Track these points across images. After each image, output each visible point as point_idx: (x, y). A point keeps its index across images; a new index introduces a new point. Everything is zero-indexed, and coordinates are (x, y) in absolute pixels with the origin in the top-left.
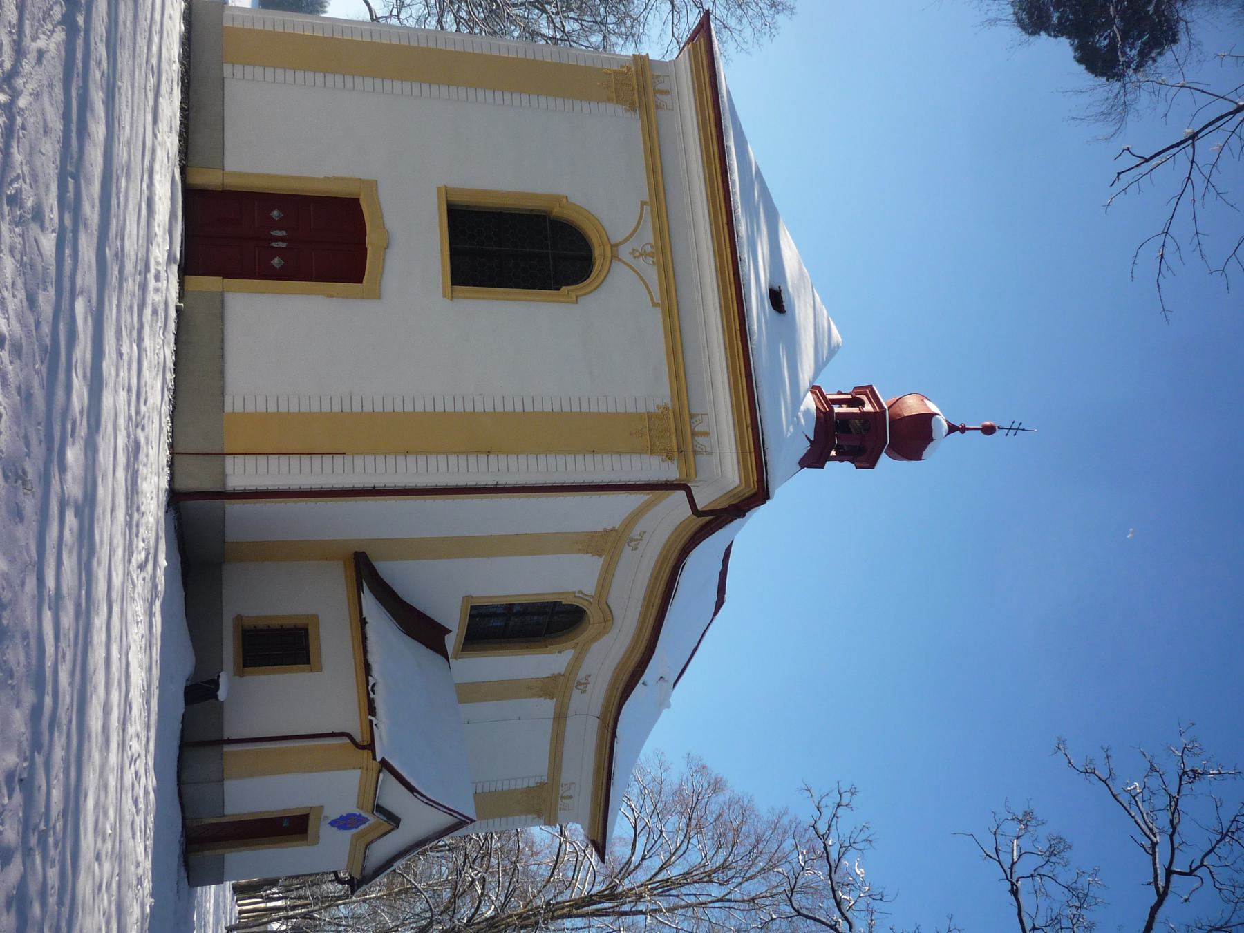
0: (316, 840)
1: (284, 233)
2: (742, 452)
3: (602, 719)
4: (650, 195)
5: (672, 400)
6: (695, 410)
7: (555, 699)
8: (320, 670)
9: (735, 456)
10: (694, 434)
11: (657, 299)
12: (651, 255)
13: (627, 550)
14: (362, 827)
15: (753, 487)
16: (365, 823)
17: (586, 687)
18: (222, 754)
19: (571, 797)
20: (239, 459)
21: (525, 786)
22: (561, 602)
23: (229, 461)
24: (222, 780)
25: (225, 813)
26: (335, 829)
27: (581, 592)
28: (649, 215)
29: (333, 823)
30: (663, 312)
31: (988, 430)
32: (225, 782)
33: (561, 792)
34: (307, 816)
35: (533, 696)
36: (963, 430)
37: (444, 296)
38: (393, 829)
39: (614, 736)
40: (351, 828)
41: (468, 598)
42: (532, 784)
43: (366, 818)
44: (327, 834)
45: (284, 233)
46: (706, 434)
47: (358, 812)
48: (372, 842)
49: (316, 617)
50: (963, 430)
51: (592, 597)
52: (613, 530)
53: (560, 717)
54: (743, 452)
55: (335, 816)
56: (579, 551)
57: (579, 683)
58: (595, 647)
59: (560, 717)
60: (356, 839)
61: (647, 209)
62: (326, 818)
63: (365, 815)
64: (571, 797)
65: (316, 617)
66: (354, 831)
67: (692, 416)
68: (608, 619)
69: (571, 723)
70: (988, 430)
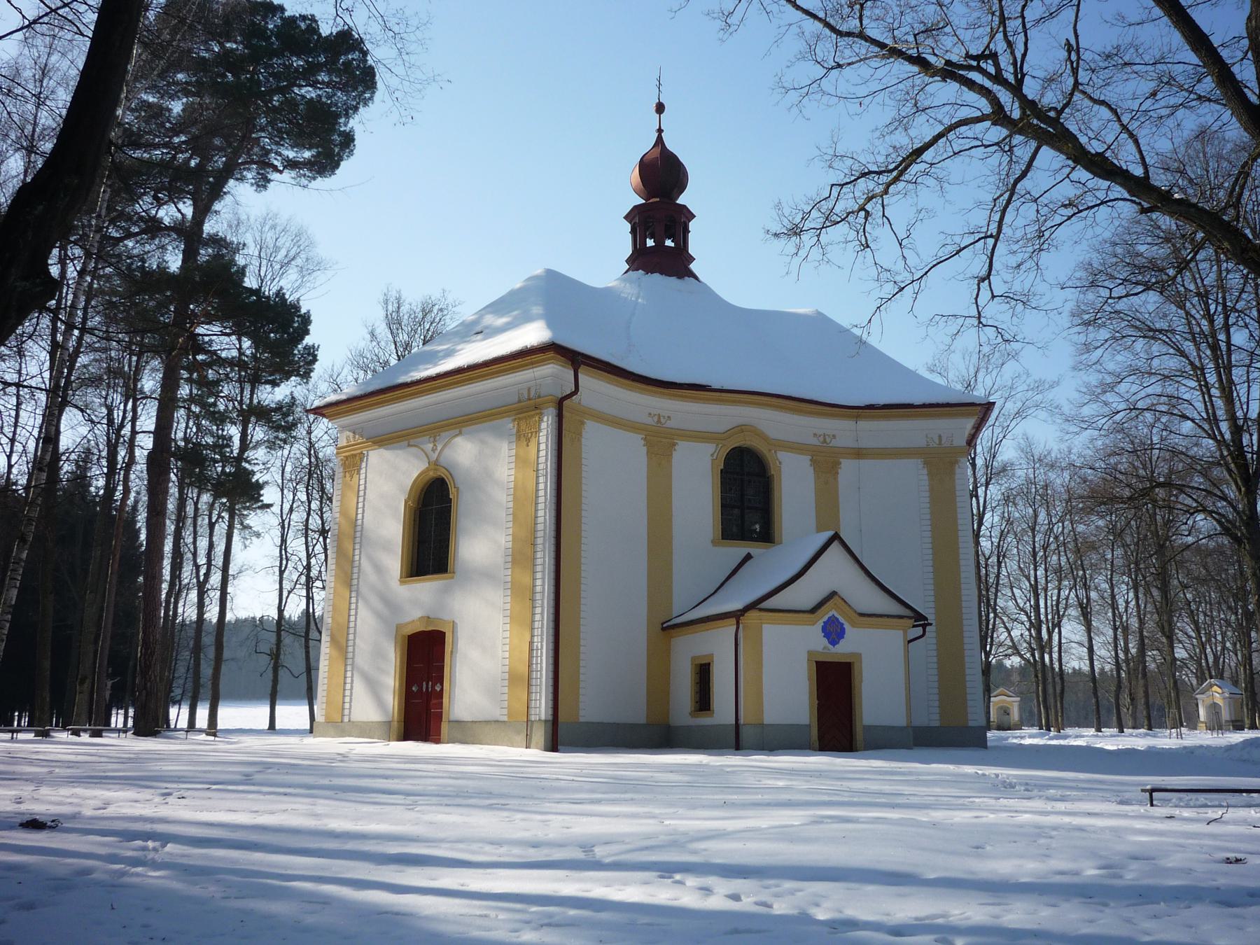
0: (859, 656)
1: (424, 683)
2: (533, 364)
3: (857, 418)
4: (424, 436)
5: (509, 416)
6: (516, 399)
7: (841, 460)
8: (712, 655)
9: (535, 369)
10: (529, 399)
11: (457, 431)
12: (435, 437)
13: (670, 424)
14: (841, 620)
15: (551, 354)
16: (837, 619)
17: (828, 435)
18: (744, 725)
19: (940, 436)
20: (532, 711)
21: (926, 477)
22: (721, 470)
23: (533, 718)
24: (762, 725)
25: (808, 723)
26: (842, 642)
27: (712, 455)
28: (415, 440)
29: (834, 643)
30: (464, 427)
31: (660, 108)
32: (766, 722)
33: (935, 445)
34: (817, 663)
35: (836, 479)
36: (660, 131)
37: (453, 578)
38: (839, 597)
39: (871, 407)
40: (843, 631)
41: (714, 543)
42: (925, 471)
43: (829, 618)
44: (843, 649)
45: (424, 683)
46: (529, 390)
47: (821, 623)
48: (855, 612)
49: (693, 659)
50: (660, 131)
51: (717, 445)
52: (645, 439)
53: (859, 454)
54: (532, 363)
55: (825, 641)
56: (670, 462)
57: (825, 441)
58: (773, 433)
59: (859, 454)
60: (854, 625)
61: (412, 442)
62: (824, 648)
63: (825, 618)
64: (940, 436)
65: (693, 659)
66: (847, 626)
67: (519, 401)
68: (741, 429)
69: (866, 443)
70: (660, 108)
